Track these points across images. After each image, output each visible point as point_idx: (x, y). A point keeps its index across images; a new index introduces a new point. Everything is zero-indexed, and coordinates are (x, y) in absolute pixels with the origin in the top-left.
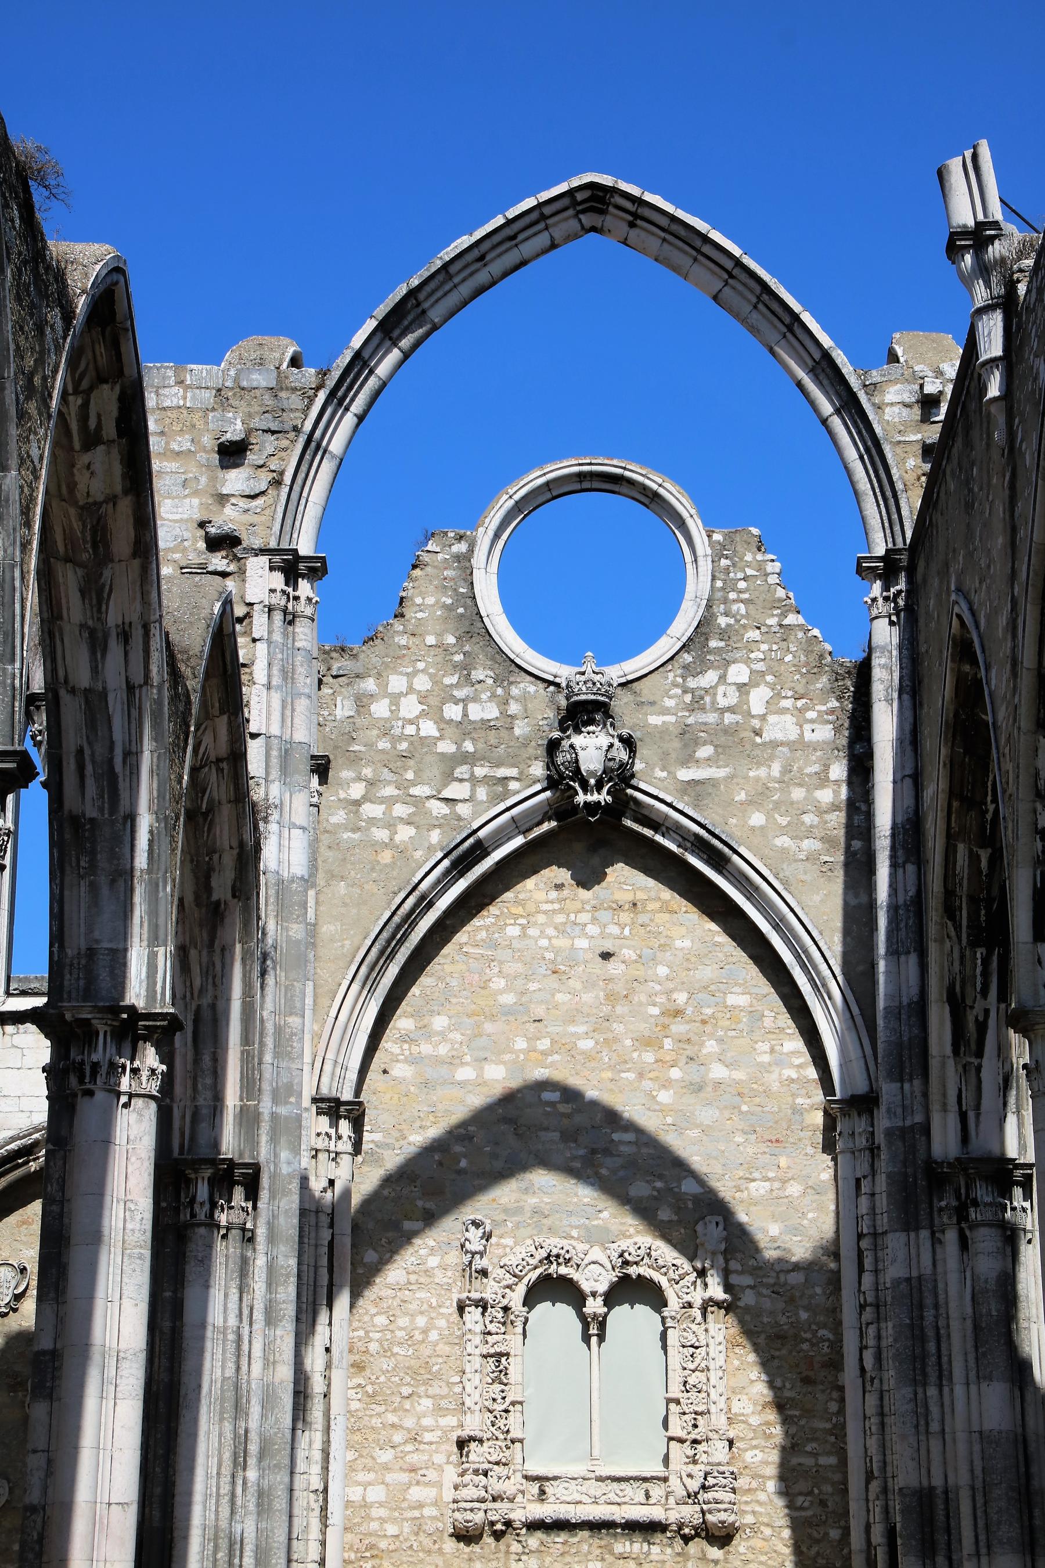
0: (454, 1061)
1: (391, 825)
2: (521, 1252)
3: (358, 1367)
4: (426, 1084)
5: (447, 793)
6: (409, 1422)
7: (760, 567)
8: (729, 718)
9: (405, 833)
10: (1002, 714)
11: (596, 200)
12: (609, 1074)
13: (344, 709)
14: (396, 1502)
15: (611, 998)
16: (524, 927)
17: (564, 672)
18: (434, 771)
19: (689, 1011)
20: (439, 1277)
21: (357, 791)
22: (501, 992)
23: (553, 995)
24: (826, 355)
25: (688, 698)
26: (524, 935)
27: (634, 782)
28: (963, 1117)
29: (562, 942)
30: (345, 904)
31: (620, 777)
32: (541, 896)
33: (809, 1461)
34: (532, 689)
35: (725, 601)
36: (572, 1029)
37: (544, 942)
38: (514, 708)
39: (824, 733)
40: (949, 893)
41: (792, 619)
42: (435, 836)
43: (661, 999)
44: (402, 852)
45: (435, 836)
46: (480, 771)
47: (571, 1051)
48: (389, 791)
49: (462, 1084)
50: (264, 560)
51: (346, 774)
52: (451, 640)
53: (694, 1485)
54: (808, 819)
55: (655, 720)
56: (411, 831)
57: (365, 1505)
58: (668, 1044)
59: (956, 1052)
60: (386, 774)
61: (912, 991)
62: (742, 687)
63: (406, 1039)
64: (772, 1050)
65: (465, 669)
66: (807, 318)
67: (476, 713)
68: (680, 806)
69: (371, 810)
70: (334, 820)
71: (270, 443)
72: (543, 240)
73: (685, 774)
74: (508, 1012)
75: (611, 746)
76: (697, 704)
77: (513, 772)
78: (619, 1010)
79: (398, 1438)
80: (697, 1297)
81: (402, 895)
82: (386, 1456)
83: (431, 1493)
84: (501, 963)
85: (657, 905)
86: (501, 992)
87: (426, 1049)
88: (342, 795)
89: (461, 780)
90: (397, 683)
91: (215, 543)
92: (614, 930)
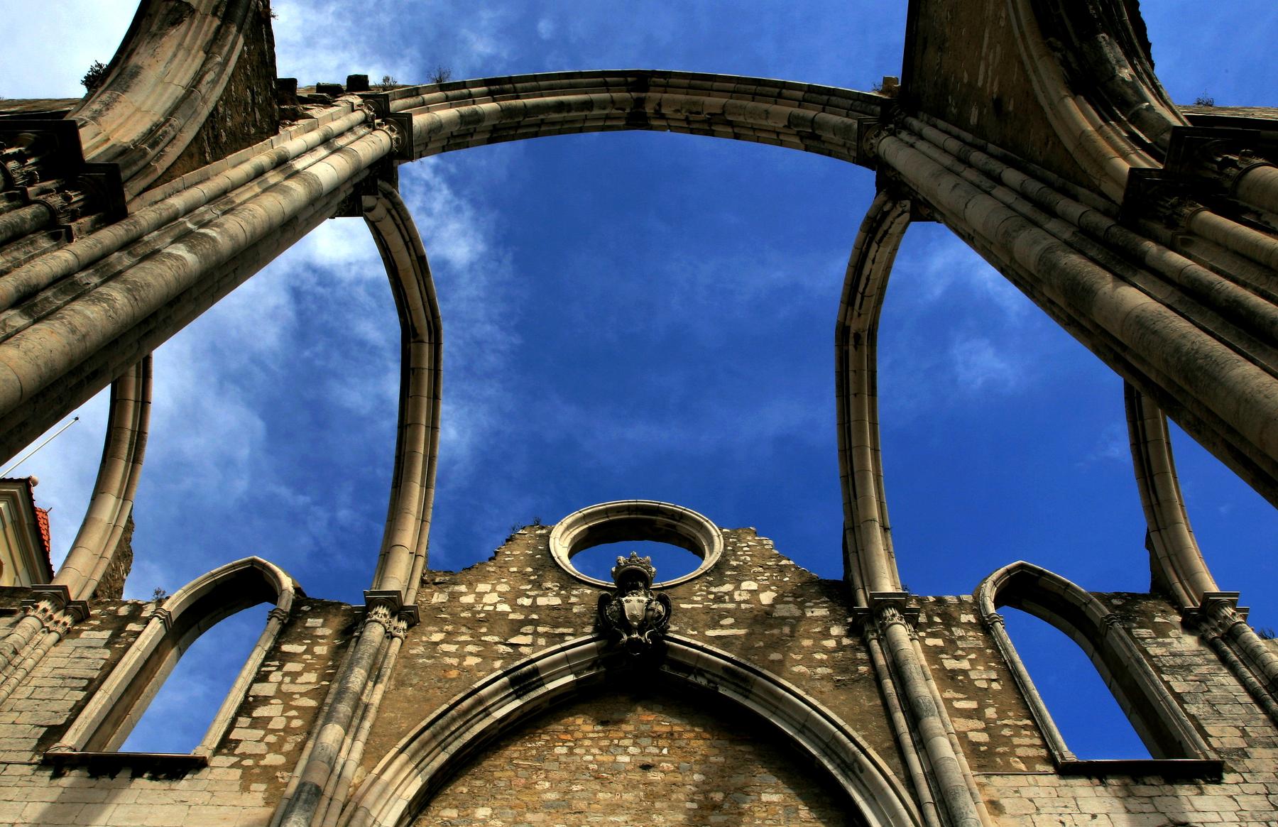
8: (743, 606)
9: (471, 661)
13: (438, 598)
15: (652, 796)
16: (571, 749)
18: (506, 629)
19: (726, 806)
21: (437, 637)
22: (545, 791)
23: (595, 794)
25: (712, 597)
27: (671, 635)
29: (606, 758)
30: (409, 701)
31: (656, 624)
32: (589, 728)
34: (589, 592)
35: (735, 555)
37: (590, 758)
38: (573, 600)
41: (784, 562)
42: (498, 664)
43: (701, 797)
44: (469, 670)
46: (540, 629)
51: (430, 628)
52: (529, 570)
54: (818, 656)
56: (478, 660)
60: (464, 629)
65: (537, 585)
67: (542, 601)
68: (710, 648)
70: (414, 652)
73: (710, 633)
74: (548, 806)
75: (649, 603)
77: (571, 630)
78: (658, 805)
81: (462, 695)
84: (547, 771)
85: (692, 735)
86: (545, 791)
88: (424, 639)
89: (526, 634)
90: (482, 587)
92: (656, 751)
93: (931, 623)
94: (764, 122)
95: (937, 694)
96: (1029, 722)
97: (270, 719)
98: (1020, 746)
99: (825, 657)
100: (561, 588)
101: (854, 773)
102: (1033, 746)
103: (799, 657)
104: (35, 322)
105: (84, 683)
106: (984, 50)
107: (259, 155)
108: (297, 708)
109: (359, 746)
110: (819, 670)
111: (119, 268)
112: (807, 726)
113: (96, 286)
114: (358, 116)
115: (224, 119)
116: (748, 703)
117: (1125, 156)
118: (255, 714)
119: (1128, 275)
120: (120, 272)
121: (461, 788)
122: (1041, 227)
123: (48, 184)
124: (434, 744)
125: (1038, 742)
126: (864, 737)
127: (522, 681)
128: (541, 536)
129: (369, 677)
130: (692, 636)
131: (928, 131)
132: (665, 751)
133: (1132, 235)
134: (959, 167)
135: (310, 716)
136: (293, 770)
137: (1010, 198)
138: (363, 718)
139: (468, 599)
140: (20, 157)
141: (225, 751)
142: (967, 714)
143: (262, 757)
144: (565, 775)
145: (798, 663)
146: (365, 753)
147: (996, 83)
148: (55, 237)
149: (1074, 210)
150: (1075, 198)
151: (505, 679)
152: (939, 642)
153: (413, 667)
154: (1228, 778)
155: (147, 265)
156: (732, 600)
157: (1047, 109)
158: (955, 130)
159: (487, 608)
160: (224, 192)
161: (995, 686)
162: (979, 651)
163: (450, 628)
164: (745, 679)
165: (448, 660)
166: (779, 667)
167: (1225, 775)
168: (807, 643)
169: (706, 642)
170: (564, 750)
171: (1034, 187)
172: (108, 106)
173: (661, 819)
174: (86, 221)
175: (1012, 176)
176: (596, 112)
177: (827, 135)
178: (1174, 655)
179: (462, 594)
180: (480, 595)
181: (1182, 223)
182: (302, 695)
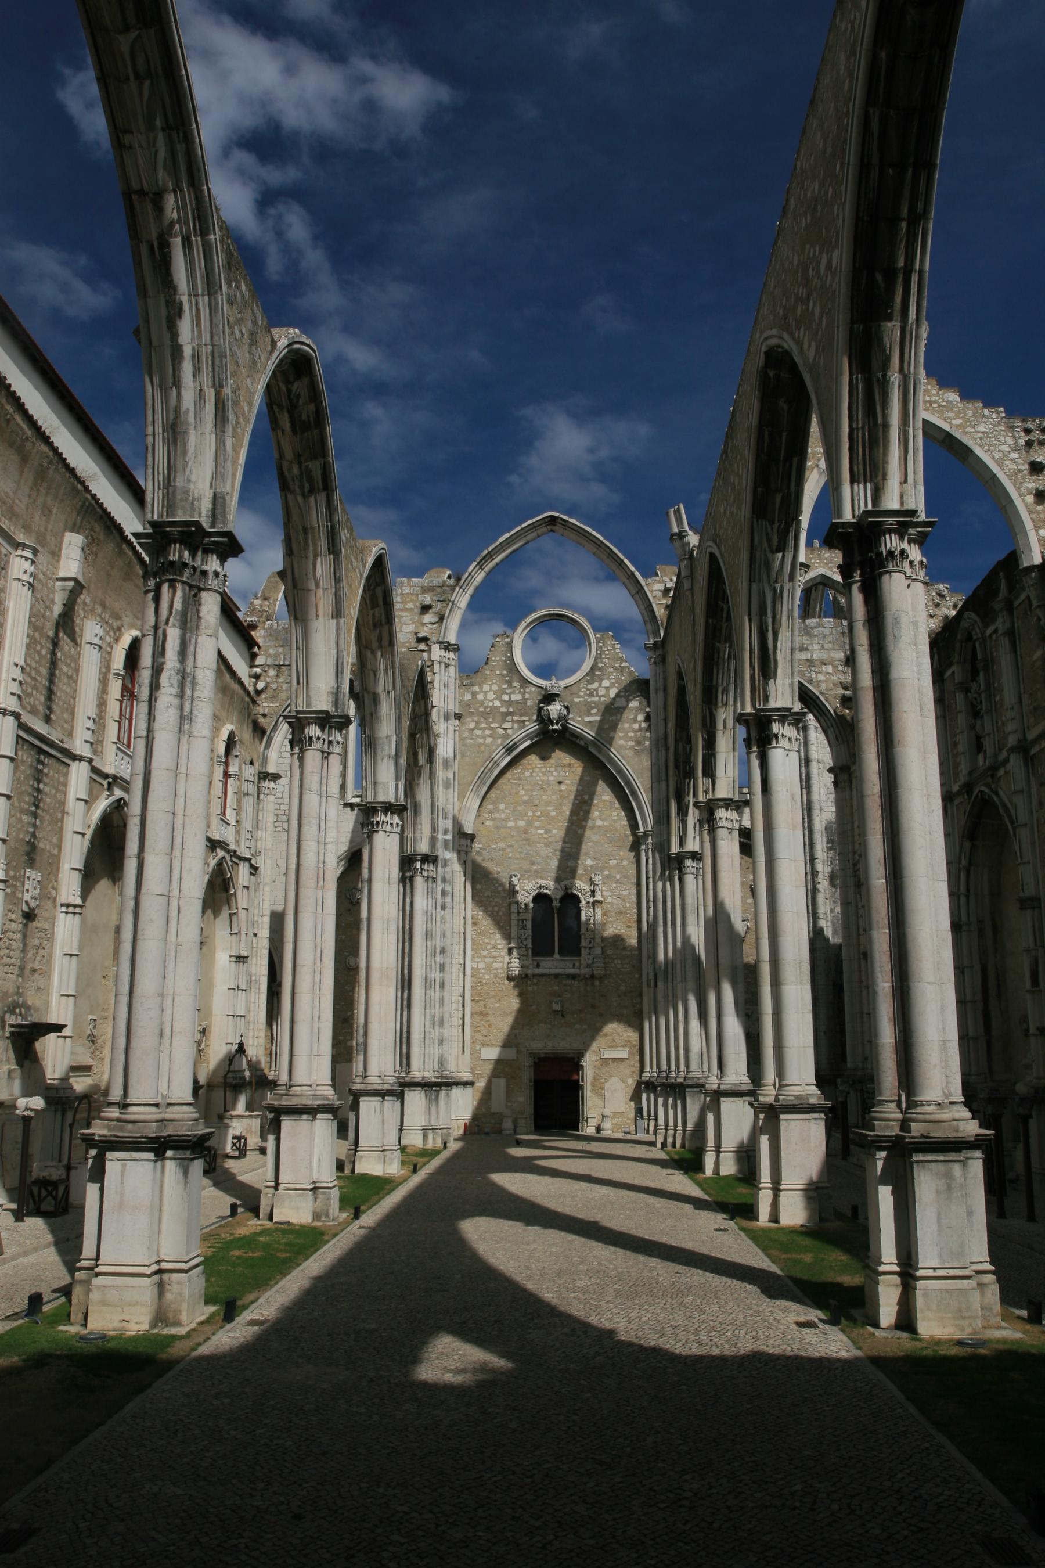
0: (507, 820)
1: (484, 738)
2: (531, 885)
3: (474, 924)
4: (497, 828)
6: (493, 942)
7: (613, 646)
8: (602, 699)
10: (692, 697)
11: (553, 520)
13: (468, 697)
14: (488, 967)
17: (543, 683)
18: (499, 718)
20: (502, 894)
21: (472, 725)
24: (633, 574)
26: (531, 775)
28: (681, 838)
33: (629, 953)
38: (527, 696)
40: (676, 760)
41: (624, 664)
44: (487, 746)
45: (499, 741)
46: (515, 718)
47: (547, 816)
48: (483, 725)
49: (510, 828)
50: (438, 645)
51: (469, 719)
53: (590, 962)
55: (576, 700)
57: (478, 968)
58: (582, 813)
59: (678, 814)
60: (482, 719)
61: (664, 794)
62: (607, 689)
63: (490, 812)
65: (509, 683)
66: (626, 561)
67: (514, 697)
69: (478, 732)
71: (439, 605)
72: (534, 534)
73: (587, 719)
74: (525, 802)
76: (591, 695)
77: (526, 718)
79: (489, 947)
80: (591, 900)
82: (485, 953)
83: (500, 965)
87: (497, 815)
90: (486, 687)
91: (420, 640)
100: (521, 687)
103: (621, 735)
109: (456, 794)
112: (620, 771)
121: (492, 794)
126: (641, 782)
139: (480, 697)
145: (621, 738)
153: (465, 745)
156: (597, 695)
163: (476, 719)
166: (610, 741)
168: (627, 725)
169: (585, 726)
179: (477, 693)
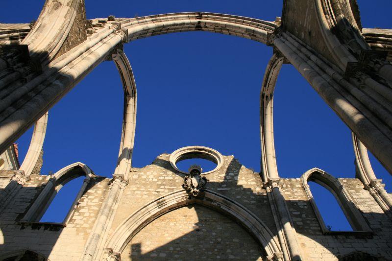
5: (157, 191)
8: (229, 181)
12: (197, 257)
16: (175, 224)
19: (222, 243)
21: (135, 189)
25: (219, 178)
36: (187, 246)
37: (181, 227)
39: (254, 183)
42: (153, 198)
43: (214, 240)
45: (153, 198)
46: (166, 187)
51: (133, 186)
54: (252, 197)
56: (147, 196)
58: (216, 250)
59: (342, 42)
60: (142, 187)
64: (247, 252)
67: (167, 178)
70: (128, 193)
73: (218, 189)
78: (201, 242)
85: (212, 221)
86: (167, 237)
90: (148, 173)
92: (201, 225)
93: (287, 187)
94: (238, 30)
95: (288, 210)
96: (315, 219)
97: (84, 213)
98: (312, 226)
99: (254, 197)
101: (261, 233)
102: (315, 226)
104: (17, 110)
105: (30, 200)
106: (306, 15)
107: (81, 48)
108: (92, 210)
109: (111, 222)
110: (252, 202)
111: (41, 90)
113: (34, 97)
114: (111, 31)
115: (71, 38)
116: (229, 211)
117: (346, 56)
118: (80, 211)
119: (346, 96)
120: (41, 91)
122: (321, 76)
123: (20, 64)
124: (133, 222)
125: (317, 225)
127: (160, 202)
128: (167, 157)
129: (114, 200)
130: (213, 190)
131: (289, 38)
132: (204, 225)
133: (347, 83)
134: (298, 52)
135: (96, 211)
136: (91, 229)
137: (313, 65)
138: (112, 214)
139: (144, 177)
140: (11, 57)
141: (71, 222)
142: (297, 216)
143: (82, 225)
144: (173, 232)
146: (112, 224)
147: (310, 26)
148: (22, 82)
149: (330, 72)
150: (331, 67)
151: (156, 203)
152: (289, 193)
154: (375, 237)
155: (49, 88)
157: (324, 38)
158: (297, 39)
159: (150, 180)
160: (71, 62)
161: (306, 207)
162: (302, 196)
164: (229, 204)
165: (138, 196)
167: (374, 236)
170: (173, 224)
171: (319, 62)
172: (36, 37)
173: (202, 246)
174: (30, 76)
175: (313, 57)
176: (186, 26)
177: (258, 35)
178: (361, 198)
179: (142, 175)
180: (148, 176)
181: (362, 81)
182: (94, 206)
